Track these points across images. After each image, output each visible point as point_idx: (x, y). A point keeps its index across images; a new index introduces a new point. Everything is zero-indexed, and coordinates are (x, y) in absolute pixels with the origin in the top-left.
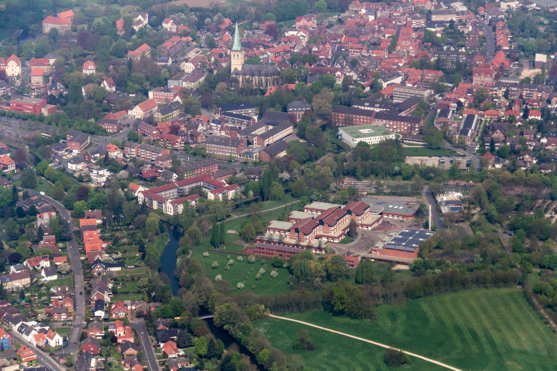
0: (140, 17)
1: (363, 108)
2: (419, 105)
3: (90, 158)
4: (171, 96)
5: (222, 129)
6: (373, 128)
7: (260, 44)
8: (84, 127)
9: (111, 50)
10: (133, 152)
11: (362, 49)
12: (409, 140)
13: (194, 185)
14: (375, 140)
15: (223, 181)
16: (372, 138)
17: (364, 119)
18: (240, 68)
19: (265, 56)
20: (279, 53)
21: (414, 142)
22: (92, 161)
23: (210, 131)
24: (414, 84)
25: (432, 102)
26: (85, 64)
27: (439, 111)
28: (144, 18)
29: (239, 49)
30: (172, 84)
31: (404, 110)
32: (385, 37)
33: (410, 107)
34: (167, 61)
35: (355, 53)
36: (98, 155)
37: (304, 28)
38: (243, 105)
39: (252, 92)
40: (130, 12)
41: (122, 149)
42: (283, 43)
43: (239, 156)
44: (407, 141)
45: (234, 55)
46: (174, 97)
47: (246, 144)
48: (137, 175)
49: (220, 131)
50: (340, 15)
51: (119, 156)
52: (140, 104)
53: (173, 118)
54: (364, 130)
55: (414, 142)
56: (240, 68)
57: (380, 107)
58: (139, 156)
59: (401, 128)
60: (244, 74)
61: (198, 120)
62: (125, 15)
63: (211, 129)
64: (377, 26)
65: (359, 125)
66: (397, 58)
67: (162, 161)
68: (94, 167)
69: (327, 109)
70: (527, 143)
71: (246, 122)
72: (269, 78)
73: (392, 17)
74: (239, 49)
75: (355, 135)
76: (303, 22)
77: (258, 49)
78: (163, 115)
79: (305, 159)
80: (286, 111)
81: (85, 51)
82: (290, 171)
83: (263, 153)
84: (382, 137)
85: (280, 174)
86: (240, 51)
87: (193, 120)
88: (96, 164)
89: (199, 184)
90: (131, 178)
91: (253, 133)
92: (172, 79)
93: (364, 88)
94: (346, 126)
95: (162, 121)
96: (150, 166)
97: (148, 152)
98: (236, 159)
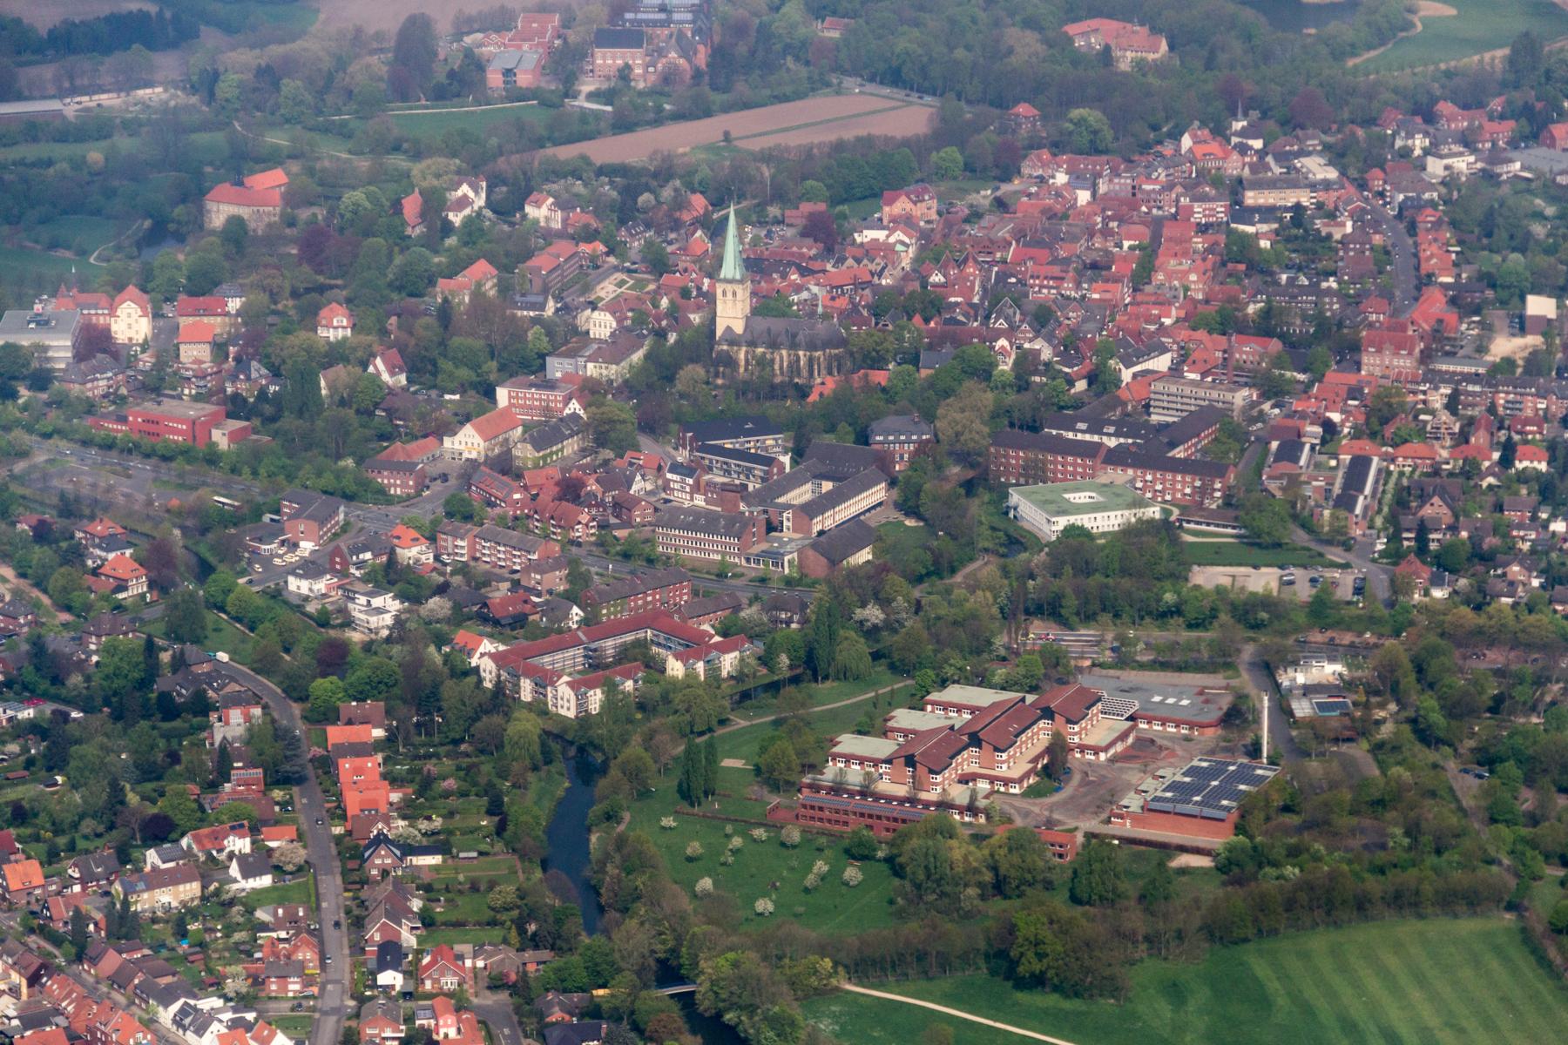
0: (465, 189)
1: (1070, 435)
2: (1220, 430)
3: (345, 564)
5: (696, 489)
6: (1103, 488)
7: (790, 264)
8: (328, 480)
9: (391, 276)
10: (460, 548)
11: (1062, 279)
12: (1198, 523)
13: (629, 638)
14: (1106, 523)
15: (706, 627)
16: (1098, 515)
17: (1075, 465)
18: (739, 328)
19: (805, 295)
21: (1212, 528)
22: (353, 570)
23: (663, 495)
24: (1204, 374)
25: (1254, 420)
26: (324, 313)
27: (1275, 445)
28: (477, 193)
29: (738, 277)
30: (557, 368)
31: (1182, 443)
32: (1121, 247)
33: (1198, 435)
34: (542, 307)
35: (1045, 291)
36: (368, 556)
37: (906, 222)
38: (750, 426)
39: (774, 392)
40: (438, 176)
41: (432, 539)
42: (850, 262)
43: (744, 562)
44: (1192, 526)
45: (724, 293)
46: (567, 401)
47: (764, 529)
48: (475, 609)
49: (692, 493)
50: (998, 188)
51: (423, 558)
52: (475, 421)
53: (563, 458)
54: (1077, 495)
55: (1212, 528)
56: (739, 328)
57: (1117, 434)
58: (476, 559)
59: (1175, 490)
60: (752, 344)
61: (631, 464)
62: (425, 184)
63: (666, 487)
64: (1099, 219)
66: (1155, 304)
67: (542, 573)
68: (359, 587)
69: (977, 437)
71: (759, 470)
72: (817, 354)
73: (1139, 196)
74: (738, 277)
75: (1053, 507)
76: (902, 206)
77: (784, 276)
78: (538, 448)
79: (924, 571)
80: (867, 443)
81: (321, 279)
82: (884, 602)
83: (811, 553)
84: (1126, 513)
85: (858, 611)
86: (741, 282)
87: (620, 464)
88: (365, 580)
89: (641, 634)
90: (459, 618)
91: (781, 500)
92: (559, 355)
93: (1071, 383)
94: (1027, 483)
95: (536, 466)
96: (507, 585)
97: (502, 549)
98: (738, 570)
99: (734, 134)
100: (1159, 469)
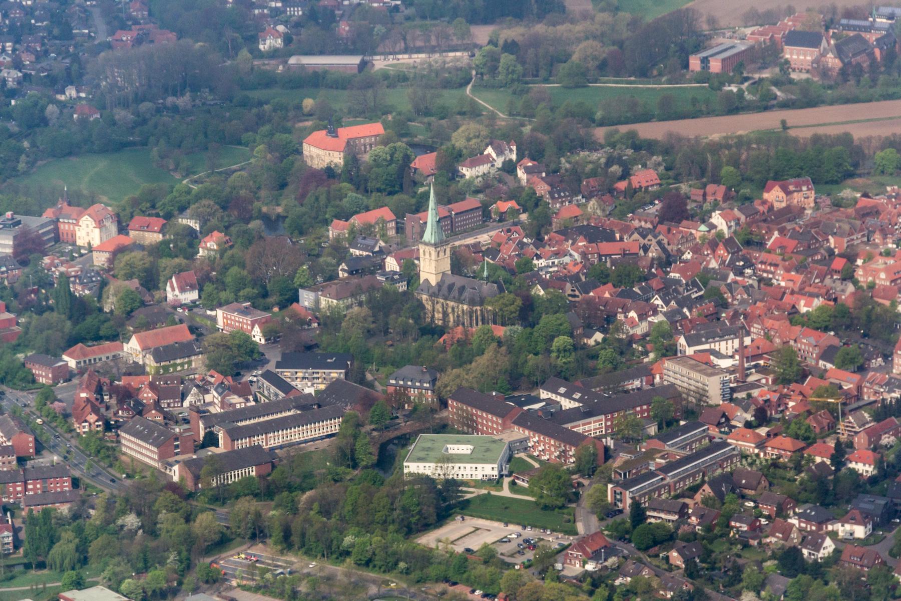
4: (247, 324)
14: (474, 472)
17: (493, 422)
19: (567, 259)
20: (610, 255)
28: (500, 152)
29: (433, 242)
54: (456, 446)
65: (487, 433)
70: (733, 524)
72: (475, 308)
99: (789, 124)
100: (543, 434)
